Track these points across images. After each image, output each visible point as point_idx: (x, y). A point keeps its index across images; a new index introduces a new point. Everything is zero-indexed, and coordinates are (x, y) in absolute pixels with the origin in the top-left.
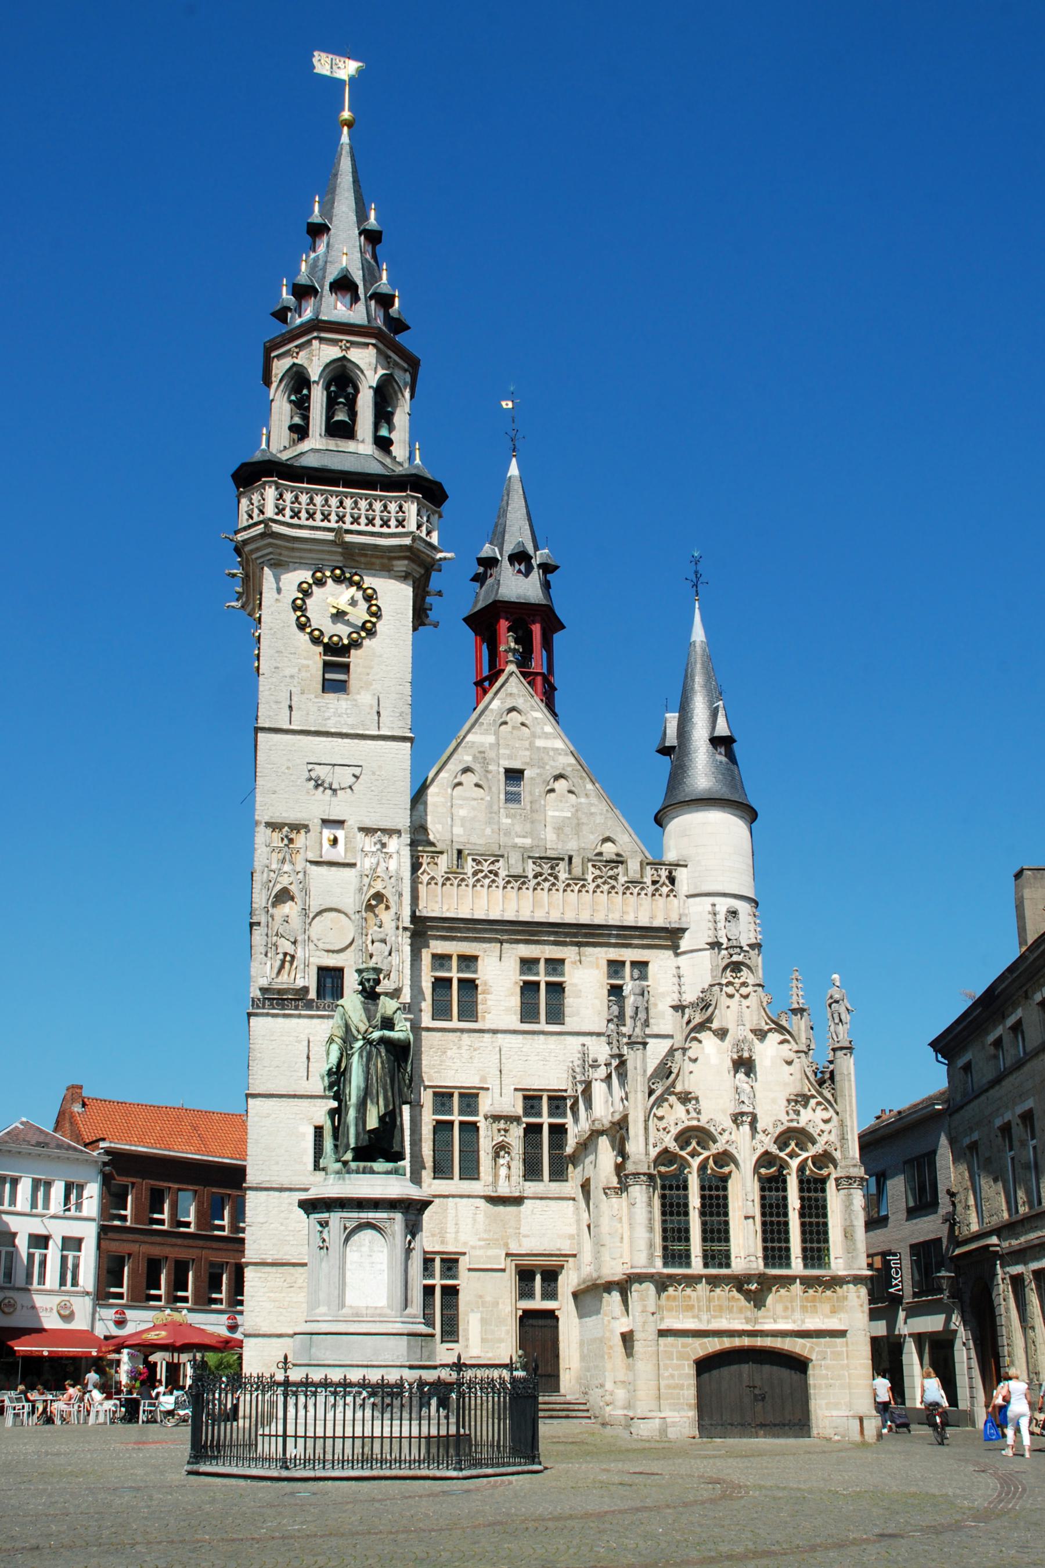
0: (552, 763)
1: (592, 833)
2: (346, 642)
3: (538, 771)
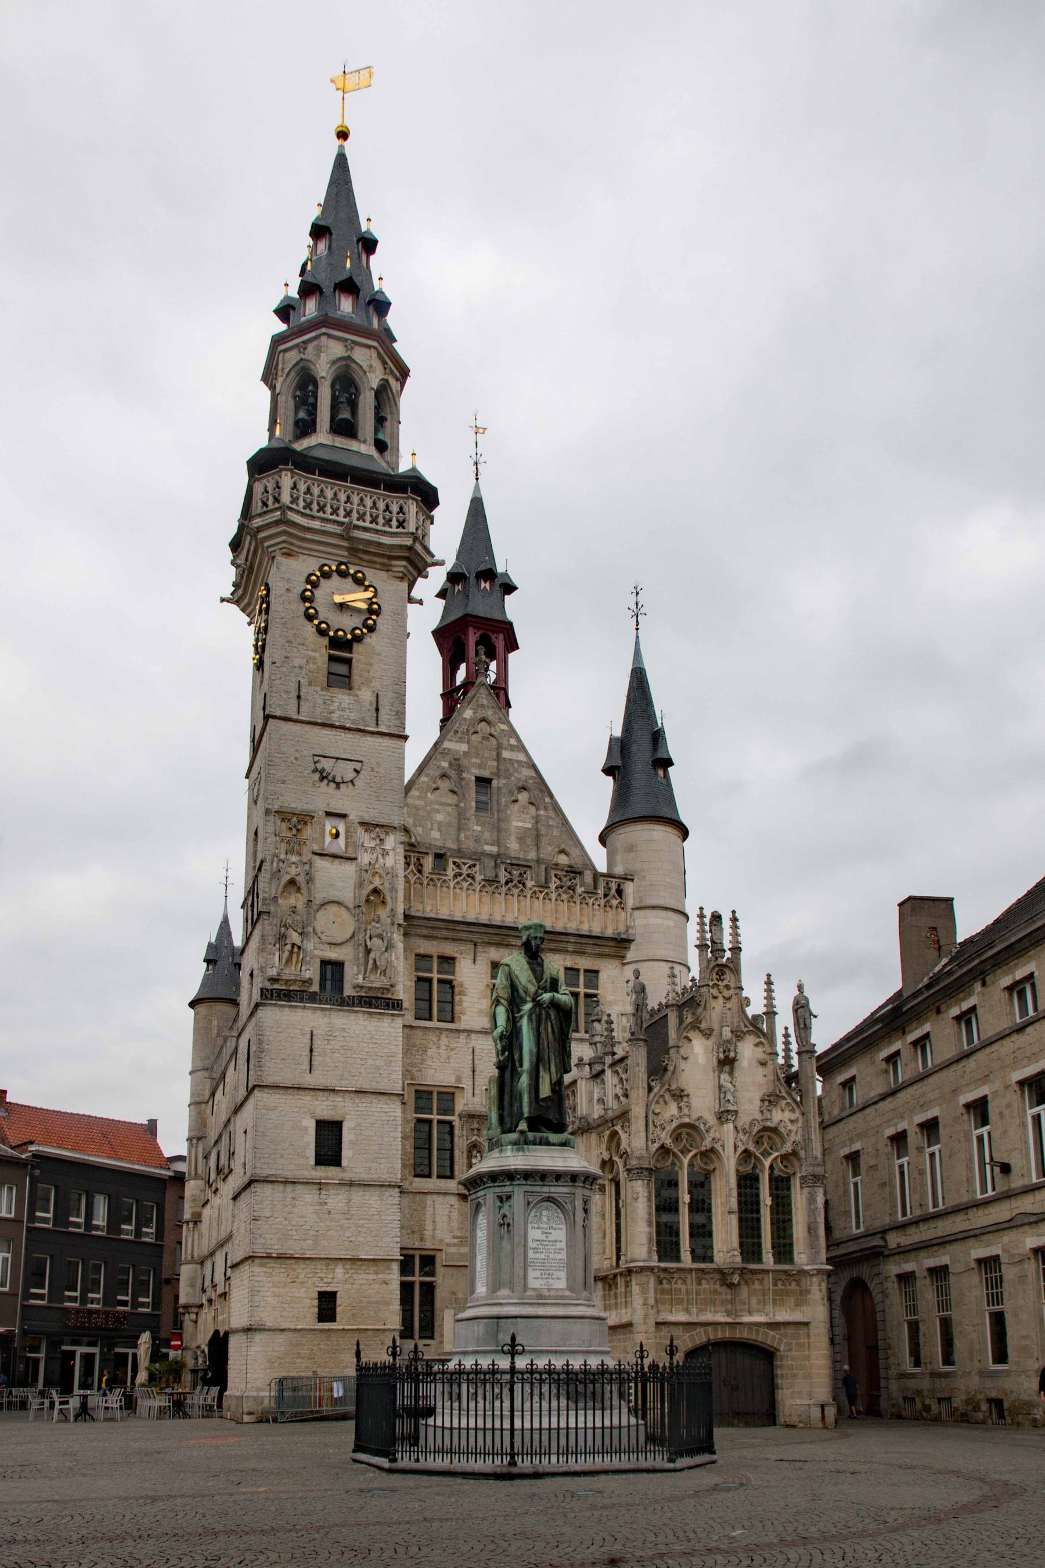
0: (516, 775)
1: (550, 845)
2: (349, 637)
3: (504, 781)
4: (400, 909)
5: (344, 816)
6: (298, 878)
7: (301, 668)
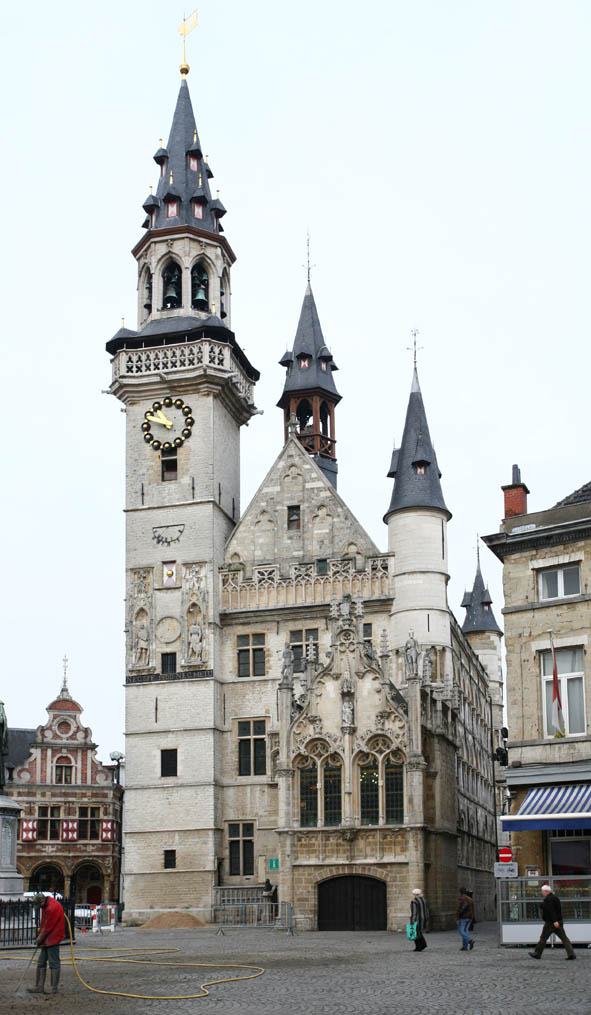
4: (211, 613)
5: (174, 562)
6: (145, 607)
7: (143, 475)
